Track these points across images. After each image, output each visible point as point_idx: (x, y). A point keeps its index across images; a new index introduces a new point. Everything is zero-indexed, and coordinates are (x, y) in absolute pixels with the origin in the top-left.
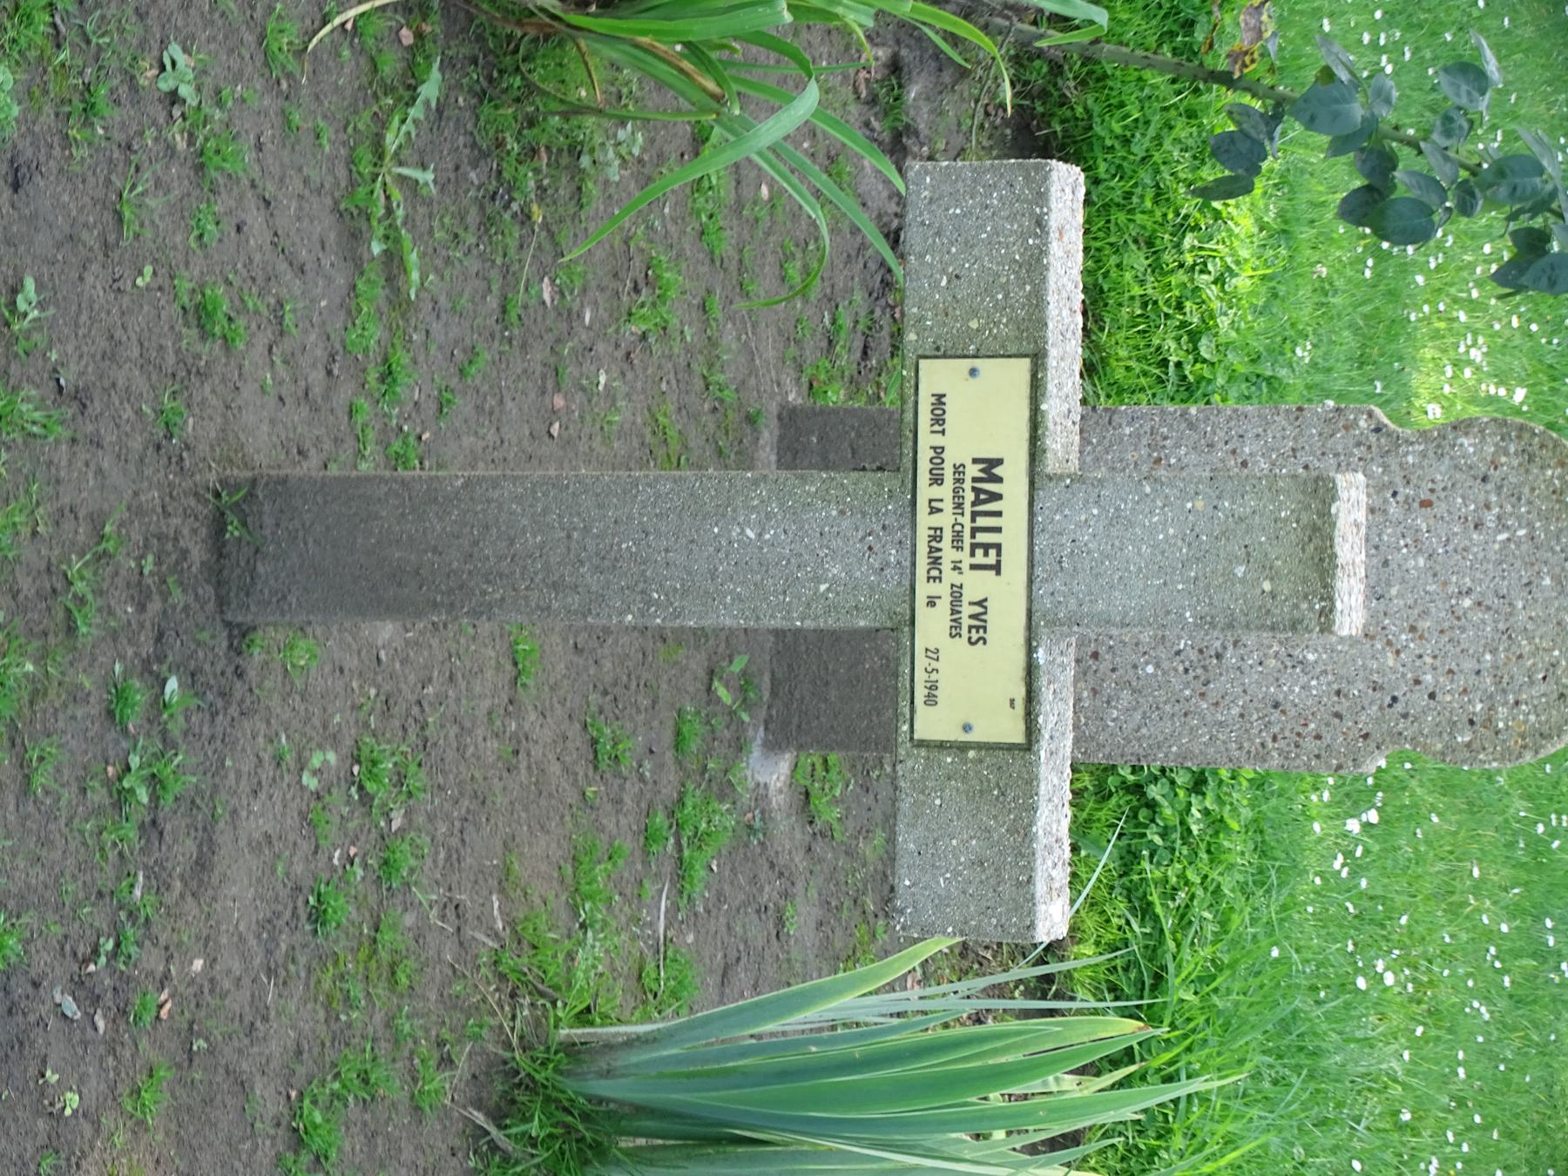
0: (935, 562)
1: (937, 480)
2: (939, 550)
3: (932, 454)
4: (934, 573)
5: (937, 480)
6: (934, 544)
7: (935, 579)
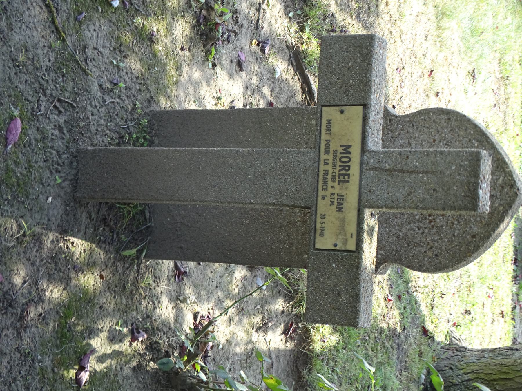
0: (325, 183)
1: (327, 152)
2: (327, 178)
3: (326, 143)
4: (325, 187)
5: (327, 152)
6: (325, 176)
7: (325, 189)
